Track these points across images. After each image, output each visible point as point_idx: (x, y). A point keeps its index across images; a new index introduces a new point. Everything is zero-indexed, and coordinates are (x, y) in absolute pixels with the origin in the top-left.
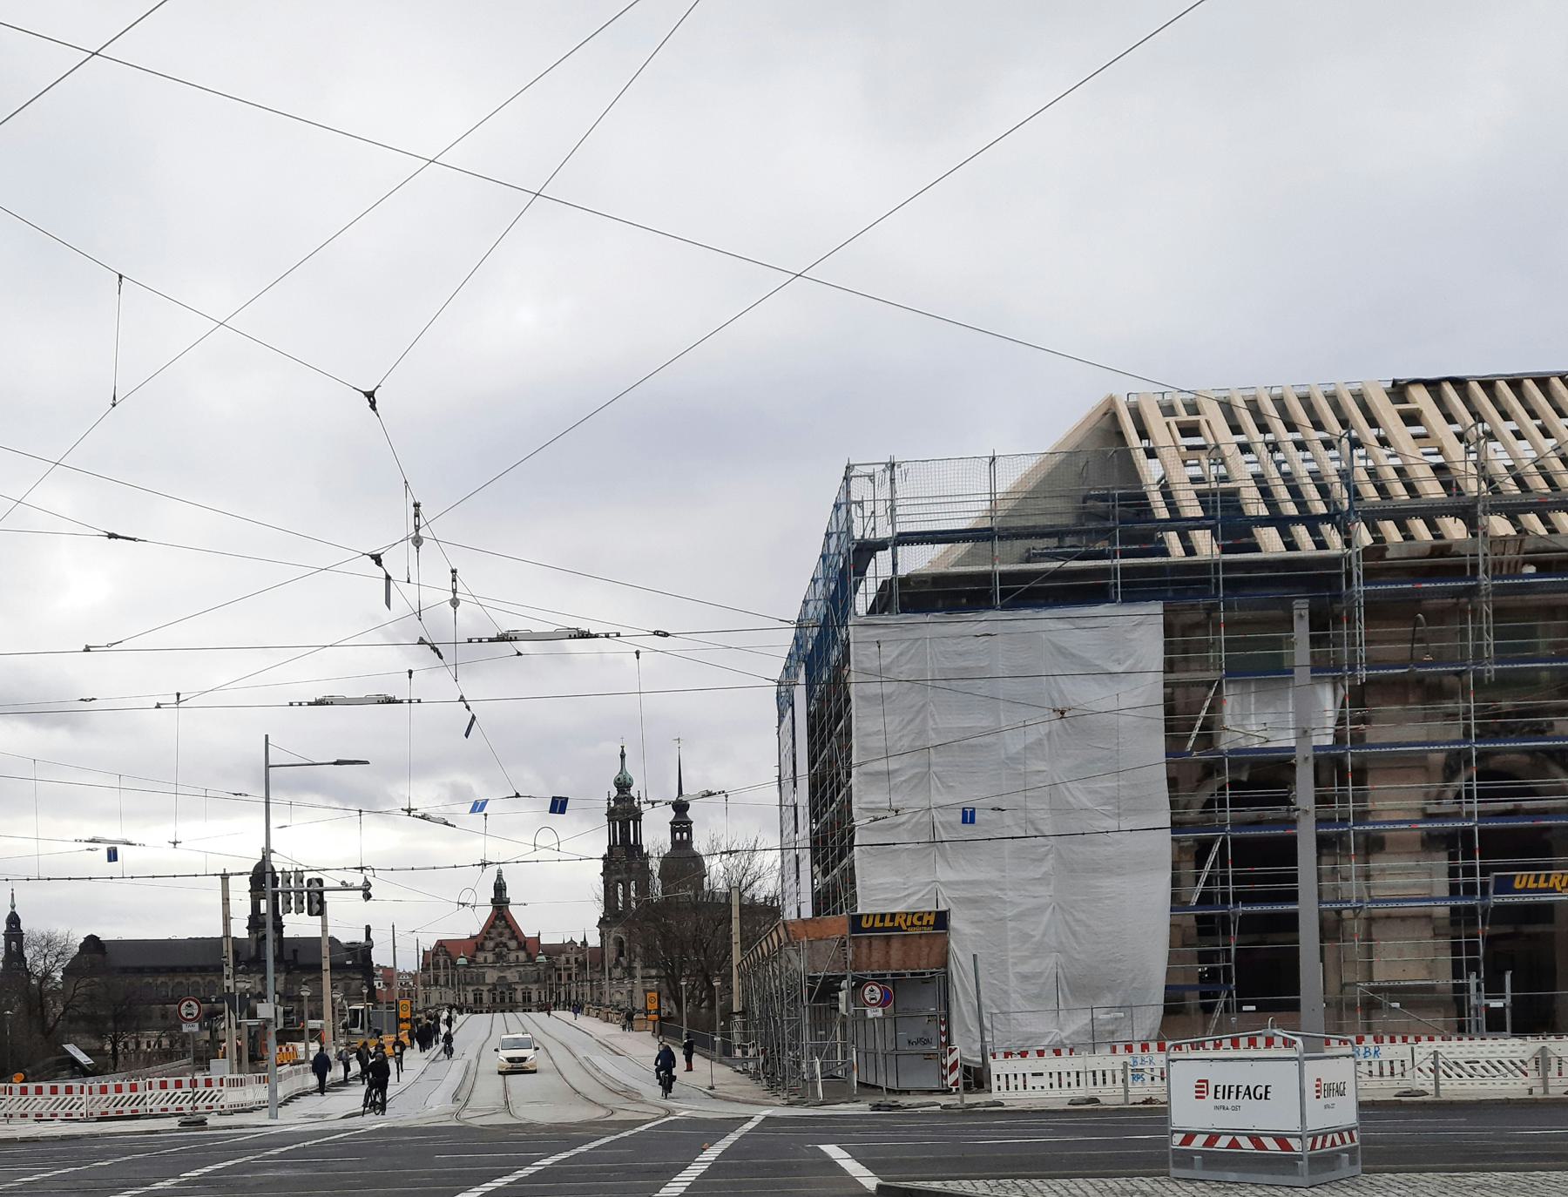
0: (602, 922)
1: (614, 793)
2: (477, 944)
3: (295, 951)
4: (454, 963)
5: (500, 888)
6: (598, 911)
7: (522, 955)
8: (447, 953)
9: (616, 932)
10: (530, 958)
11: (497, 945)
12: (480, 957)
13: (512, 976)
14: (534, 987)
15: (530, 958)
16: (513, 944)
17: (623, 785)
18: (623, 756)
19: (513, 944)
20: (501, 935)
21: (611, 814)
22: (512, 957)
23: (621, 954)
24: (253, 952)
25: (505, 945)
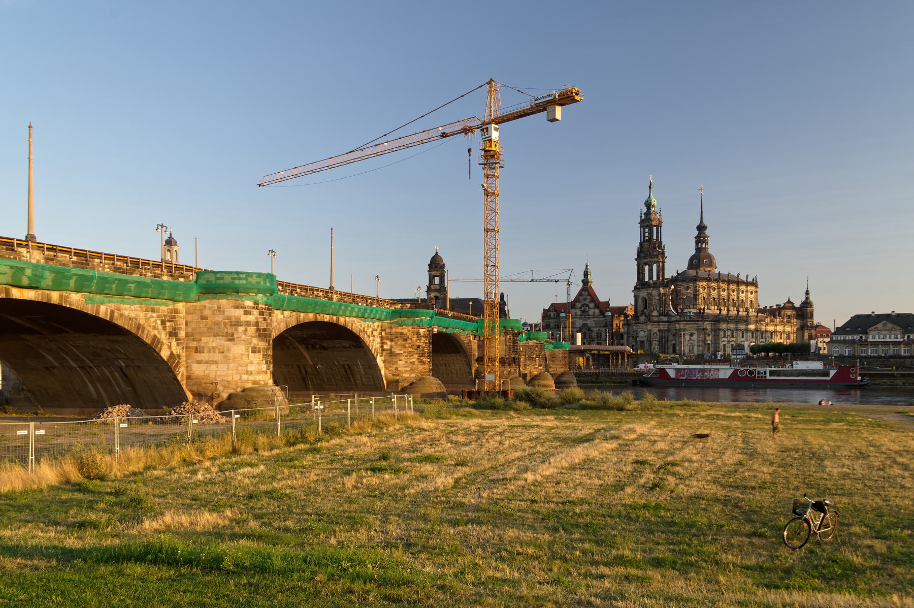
1: (645, 210)
2: (573, 305)
7: (597, 311)
9: (643, 294)
11: (583, 306)
13: (590, 322)
14: (603, 329)
16: (592, 305)
19: (592, 305)
20: (585, 300)
22: (591, 312)
23: (646, 308)
25: (587, 305)
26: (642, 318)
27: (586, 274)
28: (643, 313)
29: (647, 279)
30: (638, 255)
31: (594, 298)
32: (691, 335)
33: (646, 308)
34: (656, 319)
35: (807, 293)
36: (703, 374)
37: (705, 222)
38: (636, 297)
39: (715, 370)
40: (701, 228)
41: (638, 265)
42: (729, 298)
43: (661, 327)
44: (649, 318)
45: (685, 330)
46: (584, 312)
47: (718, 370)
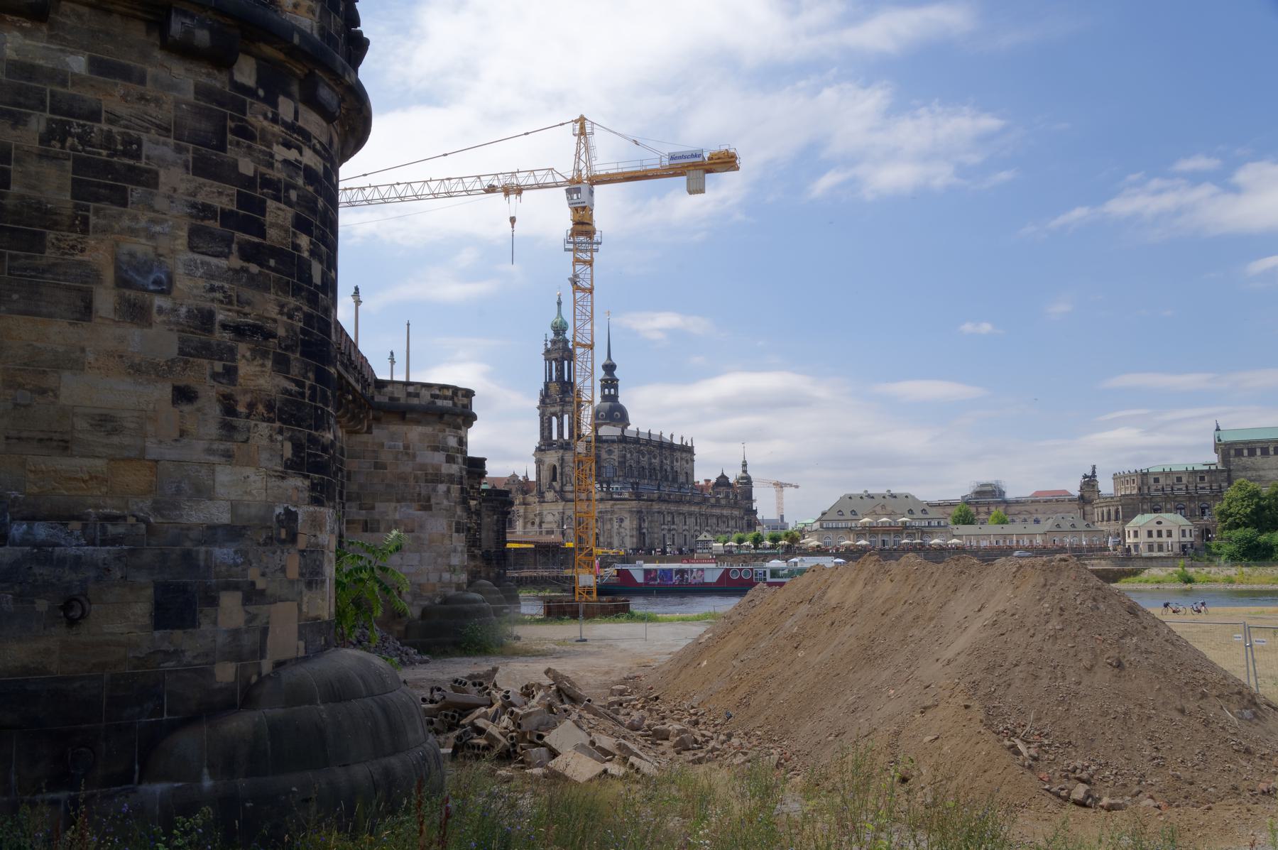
1: (551, 335)
9: (552, 458)
18: (559, 304)
23: (554, 479)
29: (555, 437)
30: (543, 402)
33: (554, 479)
34: (570, 496)
35: (745, 465)
36: (682, 576)
37: (615, 360)
38: (539, 463)
39: (698, 570)
40: (609, 368)
41: (542, 415)
42: (661, 467)
45: (613, 512)
47: (702, 570)
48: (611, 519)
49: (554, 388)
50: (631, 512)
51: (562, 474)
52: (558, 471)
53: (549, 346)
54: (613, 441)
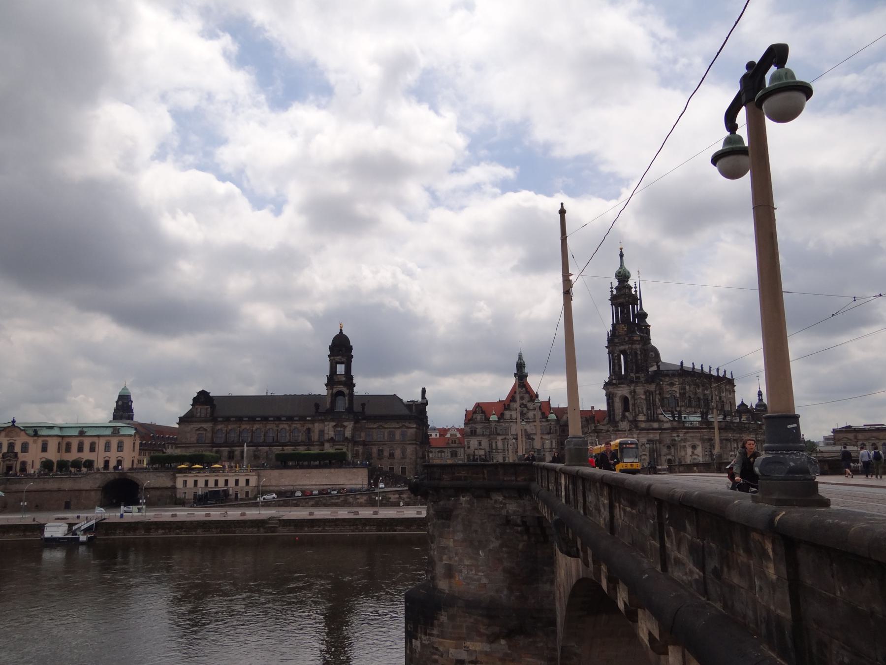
0: (607, 385)
1: (616, 283)
2: (506, 405)
3: (363, 405)
4: (487, 419)
5: (520, 366)
6: (605, 375)
7: (539, 414)
8: (483, 412)
9: (623, 391)
10: (544, 416)
12: (507, 414)
14: (547, 437)
15: (544, 416)
17: (623, 277)
18: (621, 255)
21: (614, 299)
23: (626, 408)
24: (328, 406)
25: (525, 406)
26: (624, 425)
27: (520, 366)
28: (624, 417)
30: (611, 340)
31: (534, 397)
32: (694, 447)
34: (643, 425)
43: (651, 436)
44: (634, 423)
45: (685, 440)
46: (522, 414)
48: (685, 447)
49: (623, 329)
50: (702, 440)
51: (634, 405)
52: (630, 403)
53: (614, 293)
54: (674, 375)
